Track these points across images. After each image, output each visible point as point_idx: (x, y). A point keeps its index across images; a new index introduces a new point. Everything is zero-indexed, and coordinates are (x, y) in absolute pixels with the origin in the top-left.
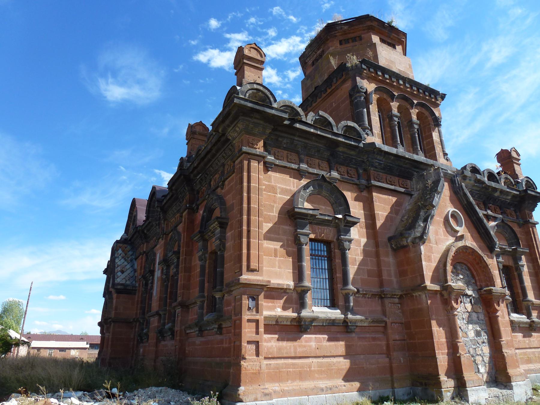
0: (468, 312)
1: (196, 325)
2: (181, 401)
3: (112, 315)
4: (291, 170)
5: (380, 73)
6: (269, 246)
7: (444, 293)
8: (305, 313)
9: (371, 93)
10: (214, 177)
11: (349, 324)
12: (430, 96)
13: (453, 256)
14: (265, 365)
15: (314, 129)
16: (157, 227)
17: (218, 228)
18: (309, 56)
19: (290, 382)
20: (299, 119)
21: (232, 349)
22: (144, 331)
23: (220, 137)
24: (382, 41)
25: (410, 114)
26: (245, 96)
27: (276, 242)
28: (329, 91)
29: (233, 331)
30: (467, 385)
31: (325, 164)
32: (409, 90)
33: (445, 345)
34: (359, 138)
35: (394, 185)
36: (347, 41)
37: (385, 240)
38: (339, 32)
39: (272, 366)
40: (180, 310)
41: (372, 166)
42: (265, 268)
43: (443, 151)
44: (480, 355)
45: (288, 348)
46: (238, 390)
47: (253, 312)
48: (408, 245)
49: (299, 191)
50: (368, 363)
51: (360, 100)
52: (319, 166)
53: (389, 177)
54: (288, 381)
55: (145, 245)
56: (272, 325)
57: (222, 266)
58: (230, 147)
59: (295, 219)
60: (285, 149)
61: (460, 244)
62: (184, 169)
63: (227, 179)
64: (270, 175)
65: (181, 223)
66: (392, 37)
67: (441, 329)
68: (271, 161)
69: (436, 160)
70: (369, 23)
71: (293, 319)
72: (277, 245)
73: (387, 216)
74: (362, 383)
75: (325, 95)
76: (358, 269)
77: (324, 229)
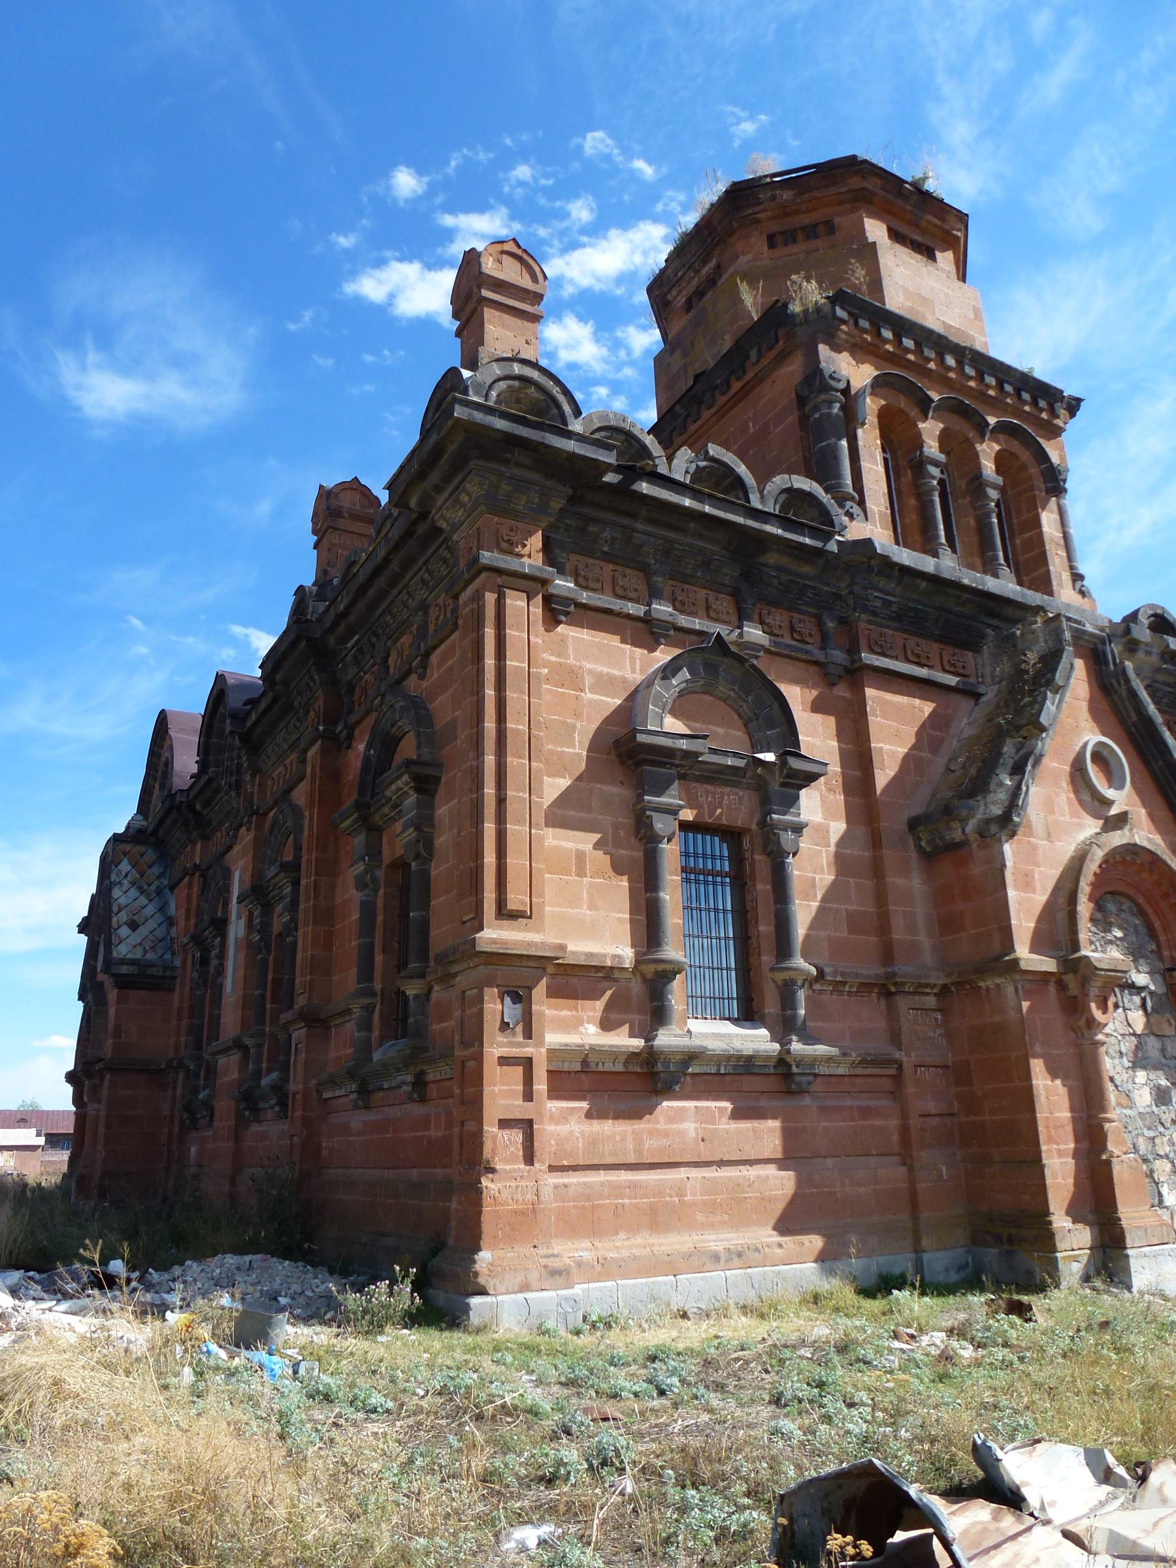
0: (1134, 1034)
1: (351, 1074)
2: (309, 1293)
3: (108, 1049)
4: (627, 622)
5: (887, 334)
6: (563, 843)
7: (1066, 978)
8: (665, 1039)
9: (861, 392)
10: (398, 645)
11: (795, 1070)
12: (1035, 403)
13: (1095, 874)
14: (551, 1190)
15: (694, 498)
16: (233, 794)
17: (411, 792)
18: (678, 281)
19: (622, 1235)
20: (648, 469)
21: (456, 1145)
22: (201, 1096)
23: (415, 523)
24: (896, 236)
25: (976, 455)
26: (487, 397)
27: (583, 834)
28: (736, 386)
29: (457, 1091)
30: (1129, 1242)
31: (724, 604)
32: (972, 384)
33: (1069, 1128)
34: (825, 526)
35: (929, 667)
36: (790, 237)
37: (902, 826)
38: (765, 210)
39: (571, 1191)
40: (304, 1031)
41: (865, 609)
42: (550, 908)
43: (1072, 568)
44: (1167, 1156)
45: (618, 1138)
46: (474, 1262)
47: (514, 1035)
48: (968, 841)
49: (648, 683)
50: (847, 1181)
51: (830, 414)
52: (708, 608)
53: (912, 642)
54: (617, 1234)
55: (199, 845)
56: (570, 1072)
57: (425, 904)
58: (444, 552)
59: (639, 764)
60: (608, 557)
61: (1117, 839)
62: (307, 620)
63: (434, 648)
64: (562, 634)
65: (301, 779)
66: (924, 224)
67: (1058, 1082)
68: (565, 594)
69: (1051, 593)
70: (855, 183)
71: (633, 1056)
72: (584, 842)
73: (906, 758)
74: (828, 1237)
75: (724, 399)
76: (821, 910)
77: (722, 793)
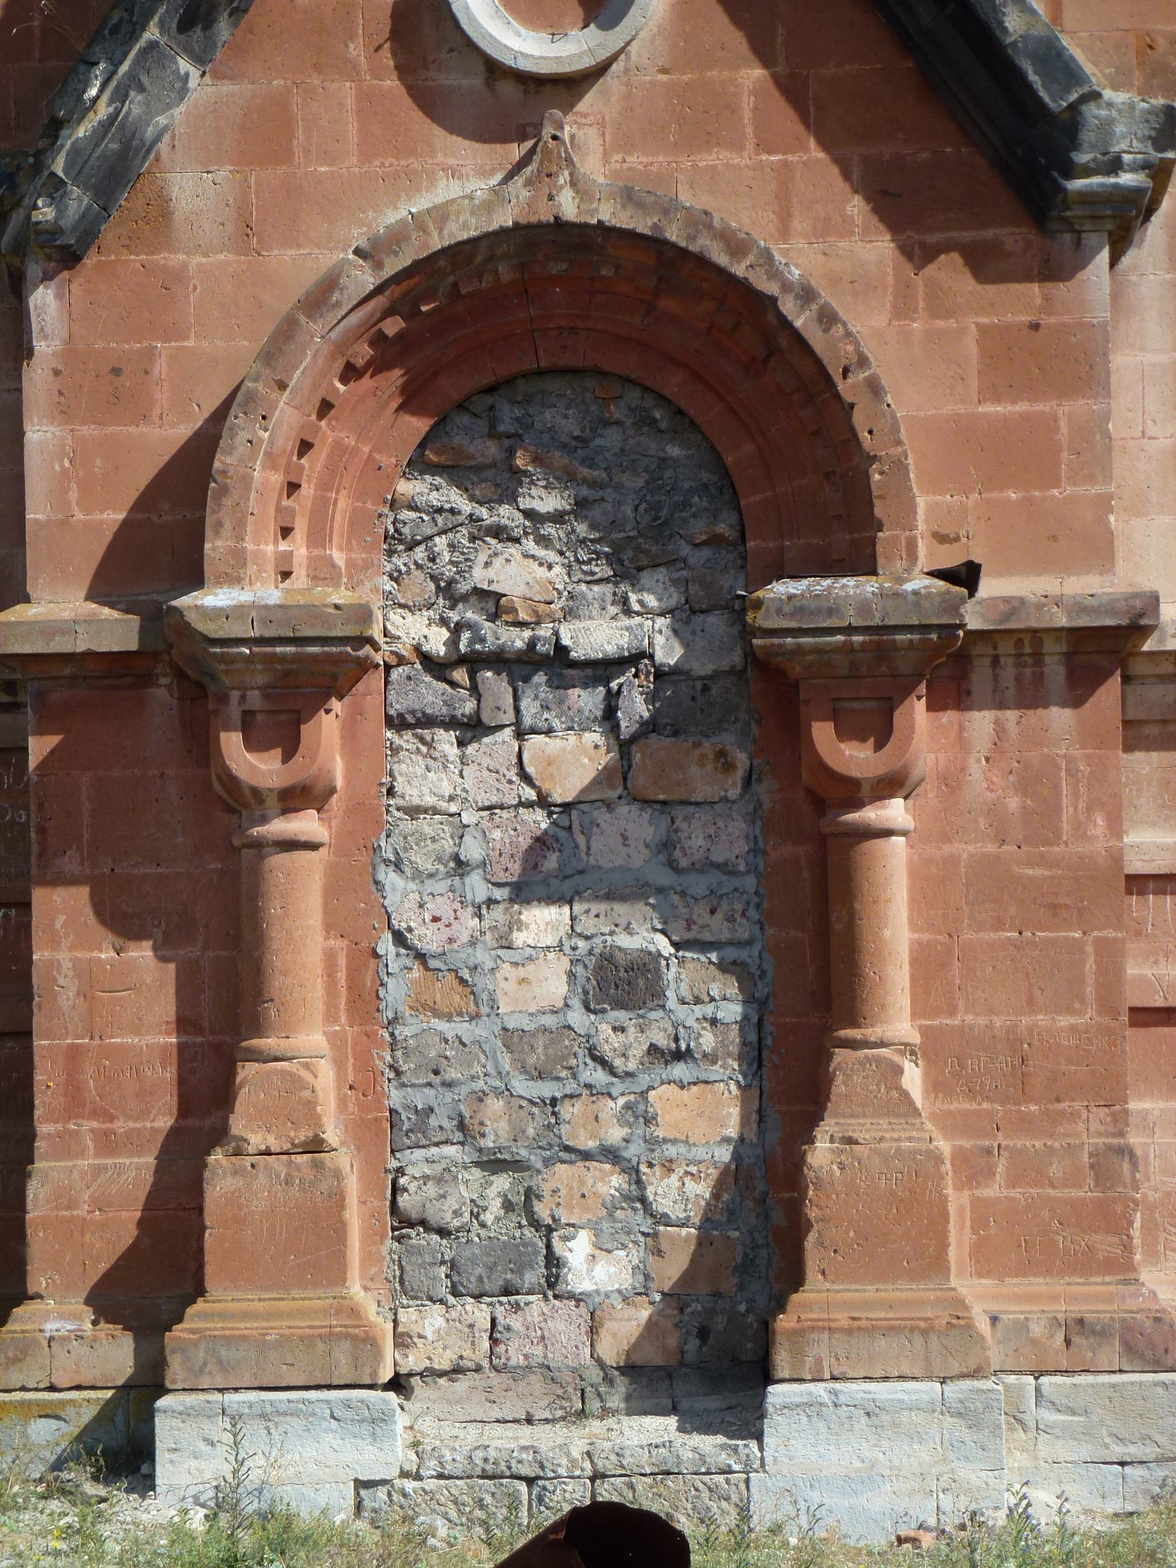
0: (543, 801)
44: (610, 1154)
